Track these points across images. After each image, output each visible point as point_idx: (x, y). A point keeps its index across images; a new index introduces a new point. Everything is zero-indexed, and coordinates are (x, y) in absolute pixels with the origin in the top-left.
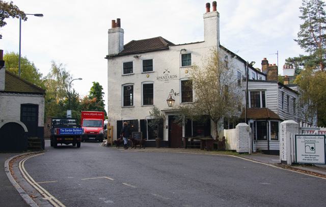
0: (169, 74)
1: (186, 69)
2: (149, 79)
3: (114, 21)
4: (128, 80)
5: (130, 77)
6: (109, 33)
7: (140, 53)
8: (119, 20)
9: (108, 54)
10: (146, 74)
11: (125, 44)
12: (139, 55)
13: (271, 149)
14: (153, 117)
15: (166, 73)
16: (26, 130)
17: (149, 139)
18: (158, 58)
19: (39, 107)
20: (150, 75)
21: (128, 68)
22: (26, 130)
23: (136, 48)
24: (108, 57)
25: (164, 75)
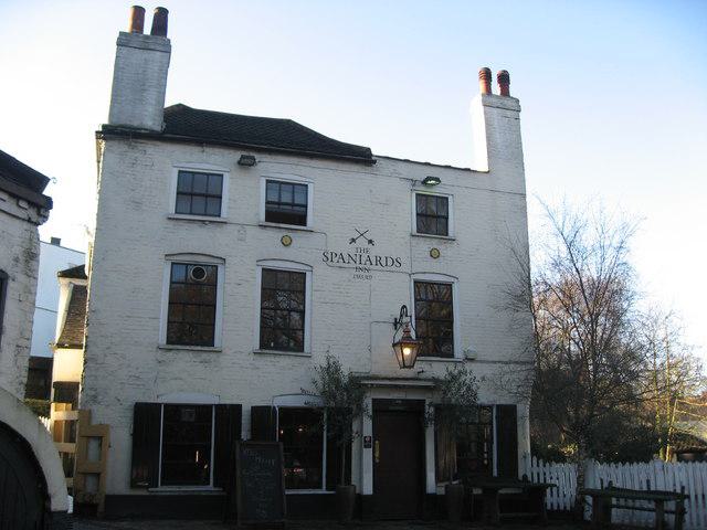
0: (374, 251)
1: (434, 244)
2: (288, 253)
3: (139, 12)
4: (197, 240)
5: (195, 226)
6: (120, 43)
7: (260, 151)
8: (162, 15)
9: (106, 122)
10: (285, 233)
11: (168, 104)
12: (257, 157)
13: (614, 510)
14: (317, 402)
15: (362, 243)
16: (495, 474)
17: (327, 489)
18: (319, 179)
19: (11, 284)
20: (299, 239)
21: (199, 197)
22: (495, 474)
23: (191, 127)
24: (108, 133)
25: (351, 250)
